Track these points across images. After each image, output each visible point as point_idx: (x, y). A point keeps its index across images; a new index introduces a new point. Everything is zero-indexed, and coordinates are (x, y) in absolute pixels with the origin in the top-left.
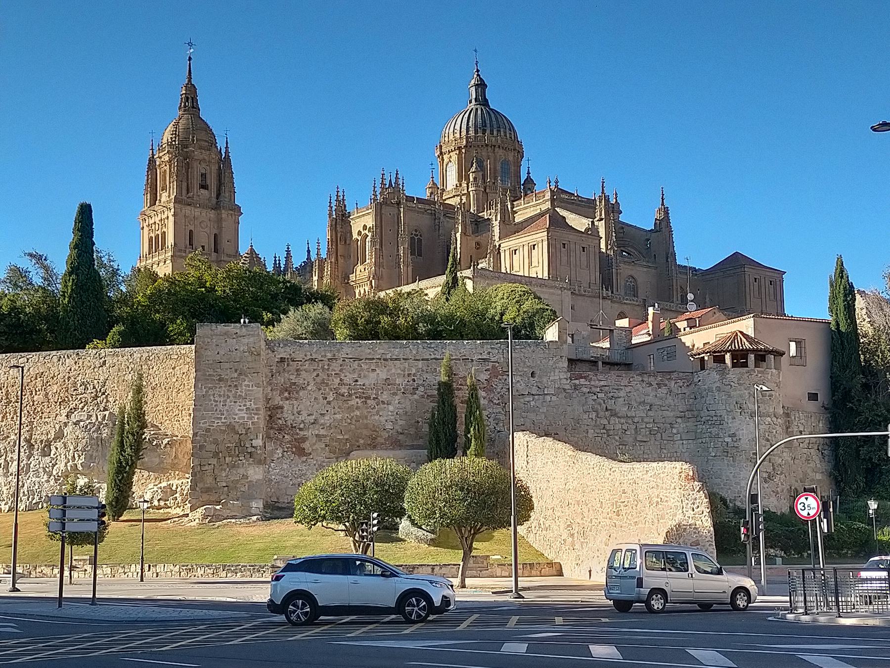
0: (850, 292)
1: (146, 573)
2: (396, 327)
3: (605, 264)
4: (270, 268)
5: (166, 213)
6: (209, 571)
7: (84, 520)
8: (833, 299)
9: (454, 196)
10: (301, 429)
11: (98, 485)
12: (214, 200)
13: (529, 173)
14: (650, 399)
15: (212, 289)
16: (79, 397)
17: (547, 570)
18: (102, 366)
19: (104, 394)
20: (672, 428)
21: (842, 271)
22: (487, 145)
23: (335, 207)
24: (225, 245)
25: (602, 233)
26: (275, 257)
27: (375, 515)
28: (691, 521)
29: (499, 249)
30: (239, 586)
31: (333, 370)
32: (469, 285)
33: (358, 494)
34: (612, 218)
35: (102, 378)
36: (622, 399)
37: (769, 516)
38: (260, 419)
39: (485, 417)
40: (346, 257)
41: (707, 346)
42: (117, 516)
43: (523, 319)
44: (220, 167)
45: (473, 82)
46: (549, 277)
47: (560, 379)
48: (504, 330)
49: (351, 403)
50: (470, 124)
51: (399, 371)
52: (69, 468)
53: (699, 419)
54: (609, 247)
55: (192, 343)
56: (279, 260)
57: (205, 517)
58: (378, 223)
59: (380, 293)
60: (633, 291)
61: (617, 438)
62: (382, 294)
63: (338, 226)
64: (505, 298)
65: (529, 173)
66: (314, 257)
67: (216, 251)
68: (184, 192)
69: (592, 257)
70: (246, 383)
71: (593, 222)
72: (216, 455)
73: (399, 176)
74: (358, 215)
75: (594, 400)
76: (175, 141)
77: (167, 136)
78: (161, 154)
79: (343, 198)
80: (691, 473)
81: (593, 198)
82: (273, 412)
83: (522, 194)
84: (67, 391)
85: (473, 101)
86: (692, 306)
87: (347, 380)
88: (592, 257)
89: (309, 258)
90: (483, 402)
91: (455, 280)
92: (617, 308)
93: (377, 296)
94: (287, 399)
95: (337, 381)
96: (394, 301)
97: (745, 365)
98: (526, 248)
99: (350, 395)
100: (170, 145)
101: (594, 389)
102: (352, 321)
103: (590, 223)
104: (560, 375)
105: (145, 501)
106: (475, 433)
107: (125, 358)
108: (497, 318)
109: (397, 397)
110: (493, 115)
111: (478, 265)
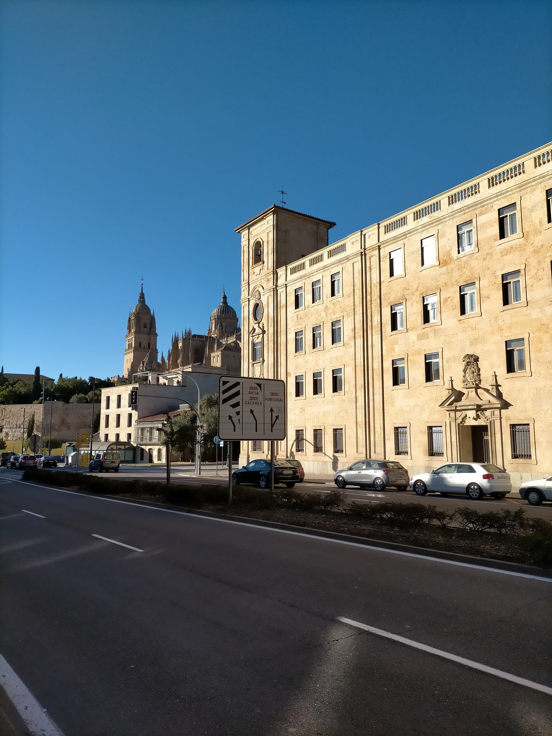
68: (138, 329)
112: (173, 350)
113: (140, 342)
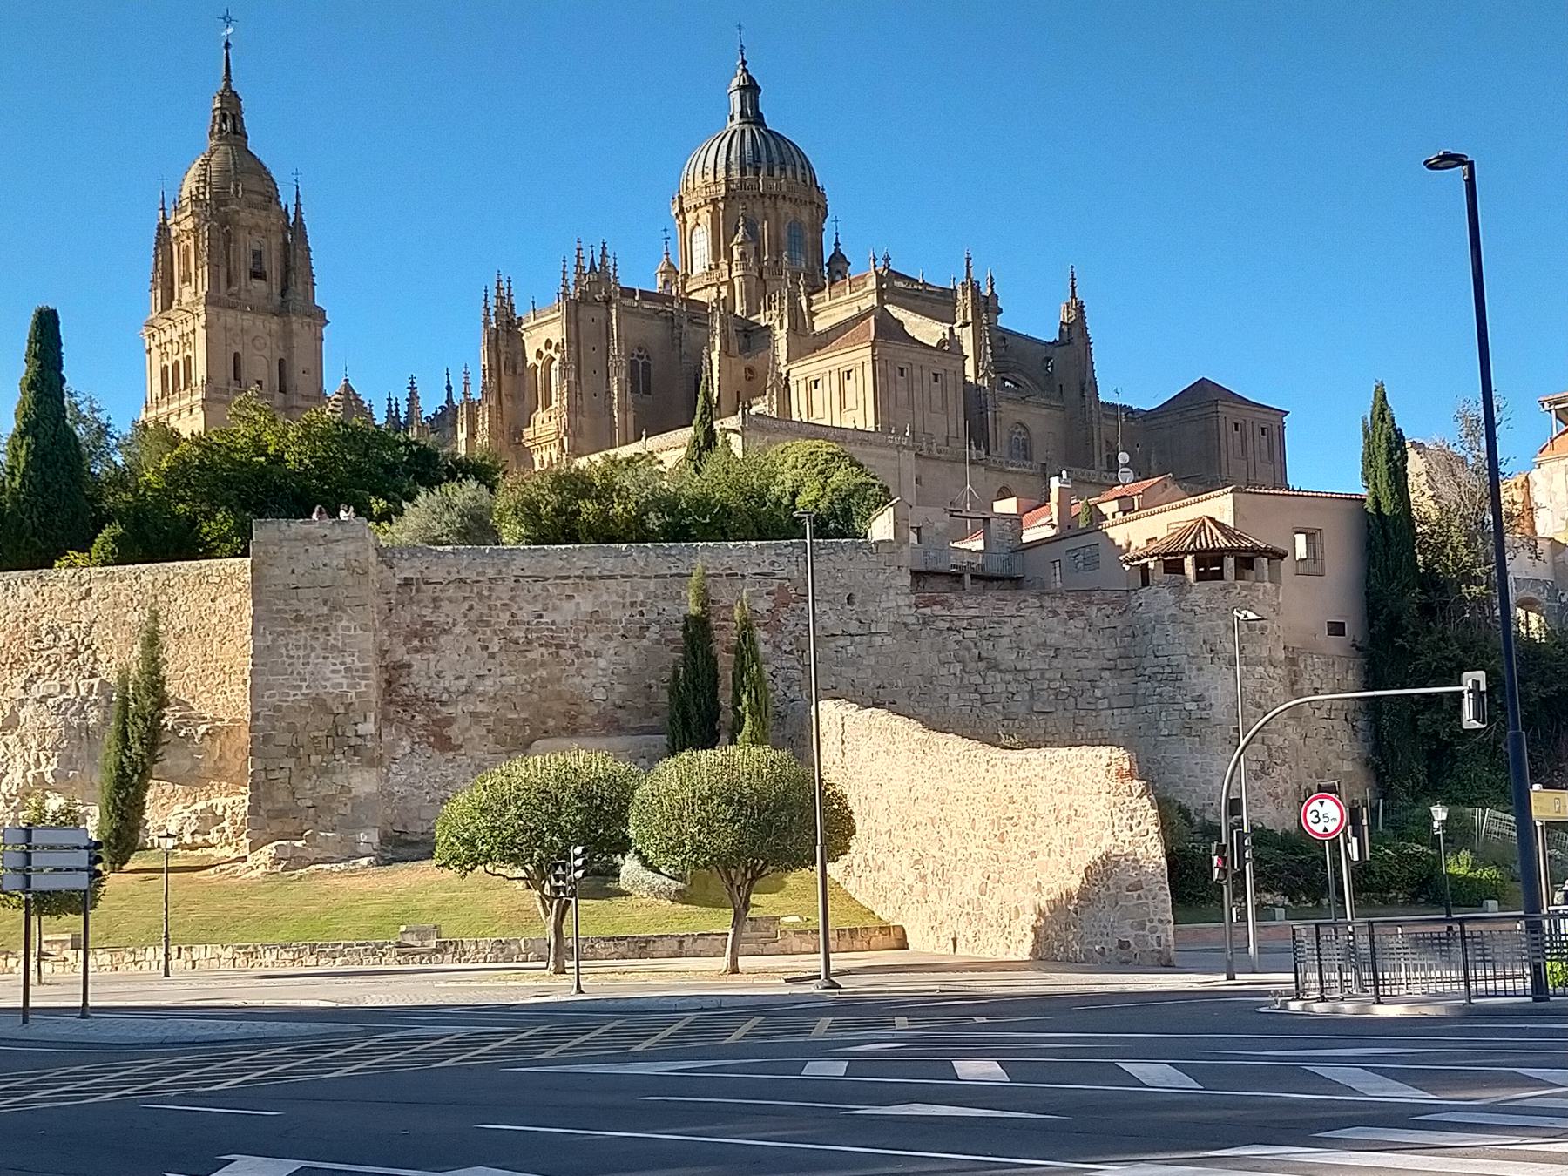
0: (1397, 445)
1: (174, 961)
2: (607, 520)
3: (974, 402)
4: (380, 419)
5: (191, 322)
6: (286, 956)
7: (60, 870)
8: (1369, 458)
9: (706, 287)
10: (443, 704)
11: (83, 810)
12: (277, 299)
13: (837, 244)
14: (1055, 639)
15: (279, 459)
16: (45, 654)
17: (879, 939)
18: (84, 599)
19: (88, 647)
20: (1094, 687)
21: (1383, 410)
22: (762, 195)
23: (495, 309)
24: (298, 379)
25: (968, 348)
26: (389, 399)
27: (579, 850)
28: (1127, 849)
29: (787, 379)
30: (340, 979)
31: (499, 598)
32: (736, 442)
33: (546, 813)
34: (985, 322)
35: (85, 620)
36: (1007, 640)
37: (1262, 837)
38: (371, 687)
39: (767, 676)
40: (516, 396)
41: (1153, 545)
42: (119, 861)
43: (831, 503)
44: (285, 239)
45: (735, 83)
46: (876, 428)
47: (899, 607)
48: (797, 523)
49: (530, 655)
50: (732, 157)
51: (615, 598)
52: (30, 780)
53: (1140, 671)
54: (981, 373)
55: (245, 554)
56: (397, 405)
57: (276, 861)
58: (573, 337)
59: (578, 460)
60: (1024, 450)
61: (999, 707)
62: (582, 462)
63: (500, 342)
64: (800, 466)
65: (837, 244)
66: (458, 398)
67: (282, 389)
68: (223, 284)
69: (950, 390)
70: (344, 623)
71: (951, 329)
72: (293, 751)
73: (608, 252)
74: (537, 322)
75: (957, 642)
76: (204, 193)
77: (190, 185)
78: (179, 218)
79: (509, 292)
80: (1127, 766)
81: (952, 287)
82: (393, 675)
83: (827, 282)
84: (22, 644)
85: (737, 116)
86: (1126, 475)
87: (523, 616)
88: (950, 390)
89: (449, 400)
90: (762, 649)
91: (710, 436)
92: (996, 480)
93: (573, 466)
94: (417, 651)
95: (506, 616)
96: (604, 475)
97: (1219, 576)
98: (835, 377)
99: (529, 642)
100: (195, 201)
101: (957, 623)
102: (529, 511)
103: (947, 332)
104: (897, 600)
105: (169, 836)
106: (750, 705)
107: (126, 582)
108: (785, 501)
109: (612, 644)
110: (772, 142)
111: (750, 407)
112: (494, 374)
113: (237, 356)
